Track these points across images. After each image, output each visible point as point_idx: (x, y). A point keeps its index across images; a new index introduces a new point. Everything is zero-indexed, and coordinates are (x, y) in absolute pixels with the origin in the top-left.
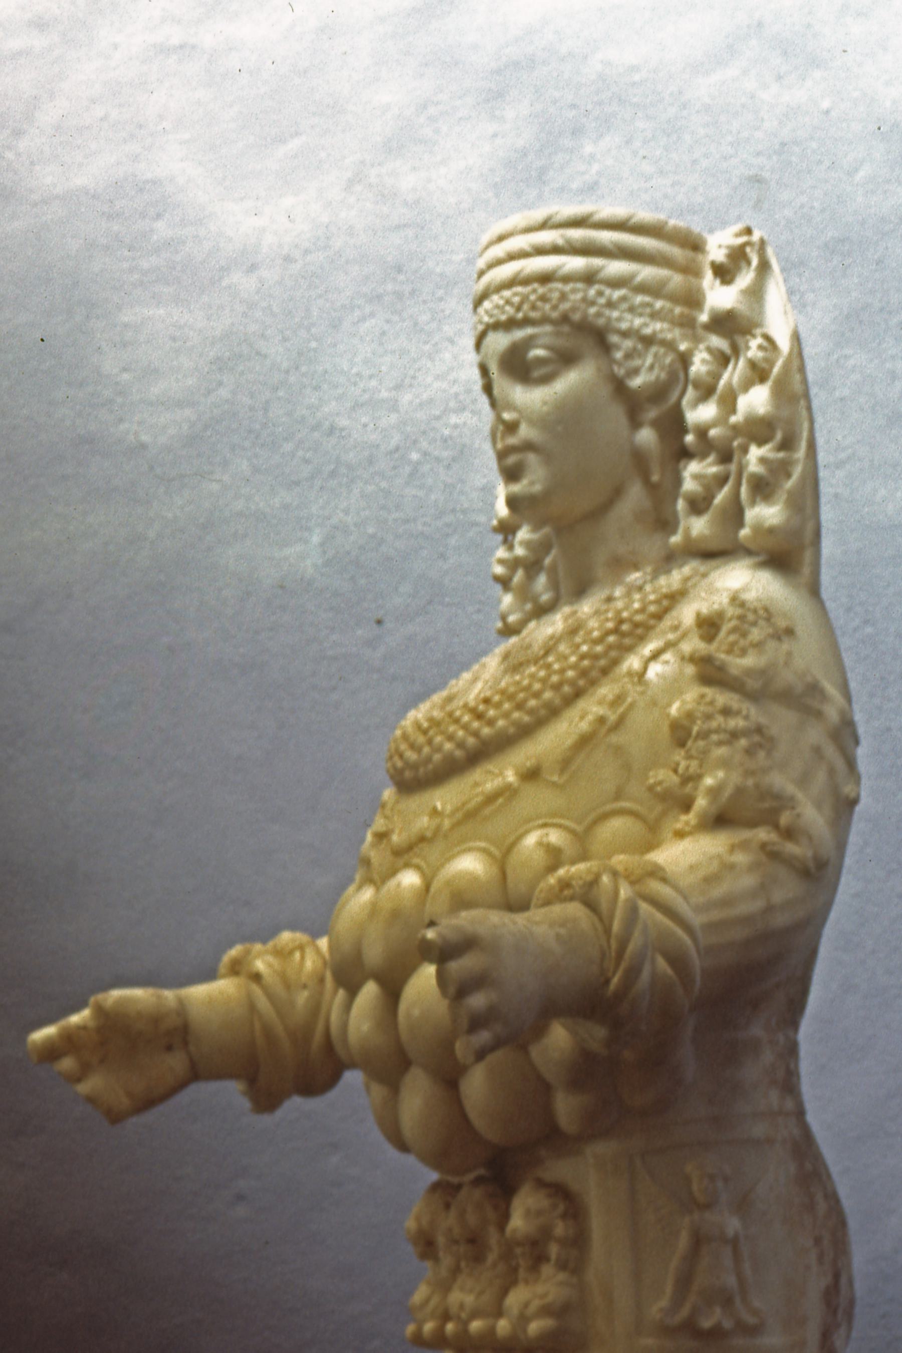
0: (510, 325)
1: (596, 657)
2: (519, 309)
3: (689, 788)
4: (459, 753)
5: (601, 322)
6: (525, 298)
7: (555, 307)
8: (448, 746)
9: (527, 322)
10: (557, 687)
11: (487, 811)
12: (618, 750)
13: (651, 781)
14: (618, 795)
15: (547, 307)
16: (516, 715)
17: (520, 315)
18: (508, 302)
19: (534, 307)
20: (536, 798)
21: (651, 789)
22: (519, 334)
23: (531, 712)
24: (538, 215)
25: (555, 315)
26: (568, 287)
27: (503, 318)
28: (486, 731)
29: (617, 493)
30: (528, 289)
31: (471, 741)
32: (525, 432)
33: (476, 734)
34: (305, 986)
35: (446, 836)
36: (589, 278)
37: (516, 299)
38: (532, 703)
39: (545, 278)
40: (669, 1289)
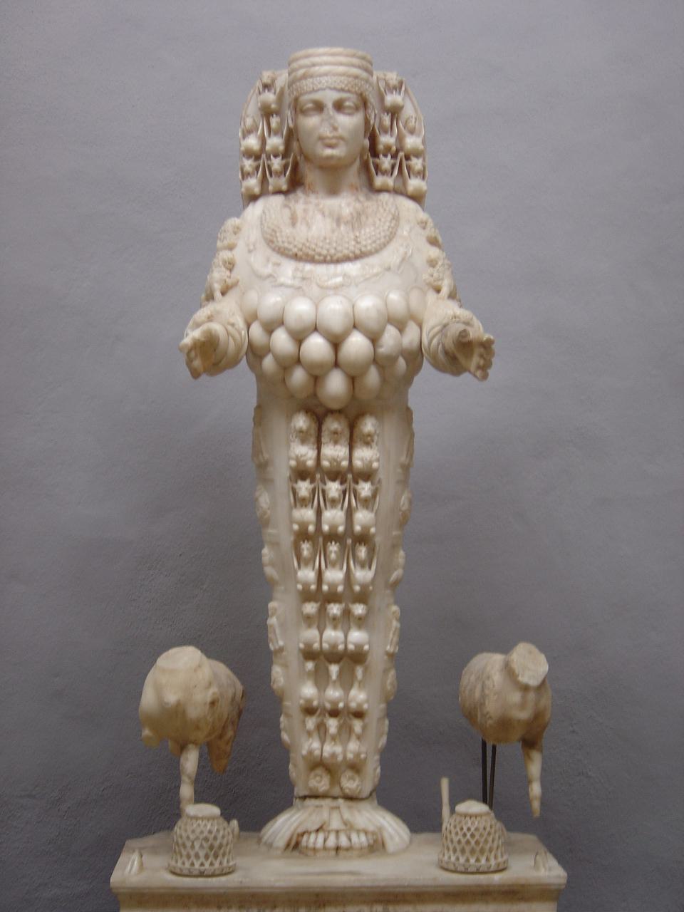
0: (342, 90)
1: (393, 228)
2: (346, 85)
3: (440, 283)
4: (351, 255)
5: (367, 97)
6: (349, 83)
7: (359, 89)
8: (346, 252)
9: (349, 91)
10: (385, 237)
13: (424, 278)
15: (357, 89)
16: (374, 245)
17: (347, 88)
18: (341, 82)
19: (352, 86)
21: (425, 281)
22: (344, 95)
23: (380, 245)
24: (360, 53)
25: (359, 92)
26: (363, 83)
27: (339, 87)
28: (363, 249)
29: (355, 160)
30: (350, 79)
31: (358, 252)
32: (340, 132)
33: (361, 250)
35: (357, 286)
36: (367, 81)
37: (346, 82)
38: (378, 242)
39: (356, 77)
40: (405, 452)
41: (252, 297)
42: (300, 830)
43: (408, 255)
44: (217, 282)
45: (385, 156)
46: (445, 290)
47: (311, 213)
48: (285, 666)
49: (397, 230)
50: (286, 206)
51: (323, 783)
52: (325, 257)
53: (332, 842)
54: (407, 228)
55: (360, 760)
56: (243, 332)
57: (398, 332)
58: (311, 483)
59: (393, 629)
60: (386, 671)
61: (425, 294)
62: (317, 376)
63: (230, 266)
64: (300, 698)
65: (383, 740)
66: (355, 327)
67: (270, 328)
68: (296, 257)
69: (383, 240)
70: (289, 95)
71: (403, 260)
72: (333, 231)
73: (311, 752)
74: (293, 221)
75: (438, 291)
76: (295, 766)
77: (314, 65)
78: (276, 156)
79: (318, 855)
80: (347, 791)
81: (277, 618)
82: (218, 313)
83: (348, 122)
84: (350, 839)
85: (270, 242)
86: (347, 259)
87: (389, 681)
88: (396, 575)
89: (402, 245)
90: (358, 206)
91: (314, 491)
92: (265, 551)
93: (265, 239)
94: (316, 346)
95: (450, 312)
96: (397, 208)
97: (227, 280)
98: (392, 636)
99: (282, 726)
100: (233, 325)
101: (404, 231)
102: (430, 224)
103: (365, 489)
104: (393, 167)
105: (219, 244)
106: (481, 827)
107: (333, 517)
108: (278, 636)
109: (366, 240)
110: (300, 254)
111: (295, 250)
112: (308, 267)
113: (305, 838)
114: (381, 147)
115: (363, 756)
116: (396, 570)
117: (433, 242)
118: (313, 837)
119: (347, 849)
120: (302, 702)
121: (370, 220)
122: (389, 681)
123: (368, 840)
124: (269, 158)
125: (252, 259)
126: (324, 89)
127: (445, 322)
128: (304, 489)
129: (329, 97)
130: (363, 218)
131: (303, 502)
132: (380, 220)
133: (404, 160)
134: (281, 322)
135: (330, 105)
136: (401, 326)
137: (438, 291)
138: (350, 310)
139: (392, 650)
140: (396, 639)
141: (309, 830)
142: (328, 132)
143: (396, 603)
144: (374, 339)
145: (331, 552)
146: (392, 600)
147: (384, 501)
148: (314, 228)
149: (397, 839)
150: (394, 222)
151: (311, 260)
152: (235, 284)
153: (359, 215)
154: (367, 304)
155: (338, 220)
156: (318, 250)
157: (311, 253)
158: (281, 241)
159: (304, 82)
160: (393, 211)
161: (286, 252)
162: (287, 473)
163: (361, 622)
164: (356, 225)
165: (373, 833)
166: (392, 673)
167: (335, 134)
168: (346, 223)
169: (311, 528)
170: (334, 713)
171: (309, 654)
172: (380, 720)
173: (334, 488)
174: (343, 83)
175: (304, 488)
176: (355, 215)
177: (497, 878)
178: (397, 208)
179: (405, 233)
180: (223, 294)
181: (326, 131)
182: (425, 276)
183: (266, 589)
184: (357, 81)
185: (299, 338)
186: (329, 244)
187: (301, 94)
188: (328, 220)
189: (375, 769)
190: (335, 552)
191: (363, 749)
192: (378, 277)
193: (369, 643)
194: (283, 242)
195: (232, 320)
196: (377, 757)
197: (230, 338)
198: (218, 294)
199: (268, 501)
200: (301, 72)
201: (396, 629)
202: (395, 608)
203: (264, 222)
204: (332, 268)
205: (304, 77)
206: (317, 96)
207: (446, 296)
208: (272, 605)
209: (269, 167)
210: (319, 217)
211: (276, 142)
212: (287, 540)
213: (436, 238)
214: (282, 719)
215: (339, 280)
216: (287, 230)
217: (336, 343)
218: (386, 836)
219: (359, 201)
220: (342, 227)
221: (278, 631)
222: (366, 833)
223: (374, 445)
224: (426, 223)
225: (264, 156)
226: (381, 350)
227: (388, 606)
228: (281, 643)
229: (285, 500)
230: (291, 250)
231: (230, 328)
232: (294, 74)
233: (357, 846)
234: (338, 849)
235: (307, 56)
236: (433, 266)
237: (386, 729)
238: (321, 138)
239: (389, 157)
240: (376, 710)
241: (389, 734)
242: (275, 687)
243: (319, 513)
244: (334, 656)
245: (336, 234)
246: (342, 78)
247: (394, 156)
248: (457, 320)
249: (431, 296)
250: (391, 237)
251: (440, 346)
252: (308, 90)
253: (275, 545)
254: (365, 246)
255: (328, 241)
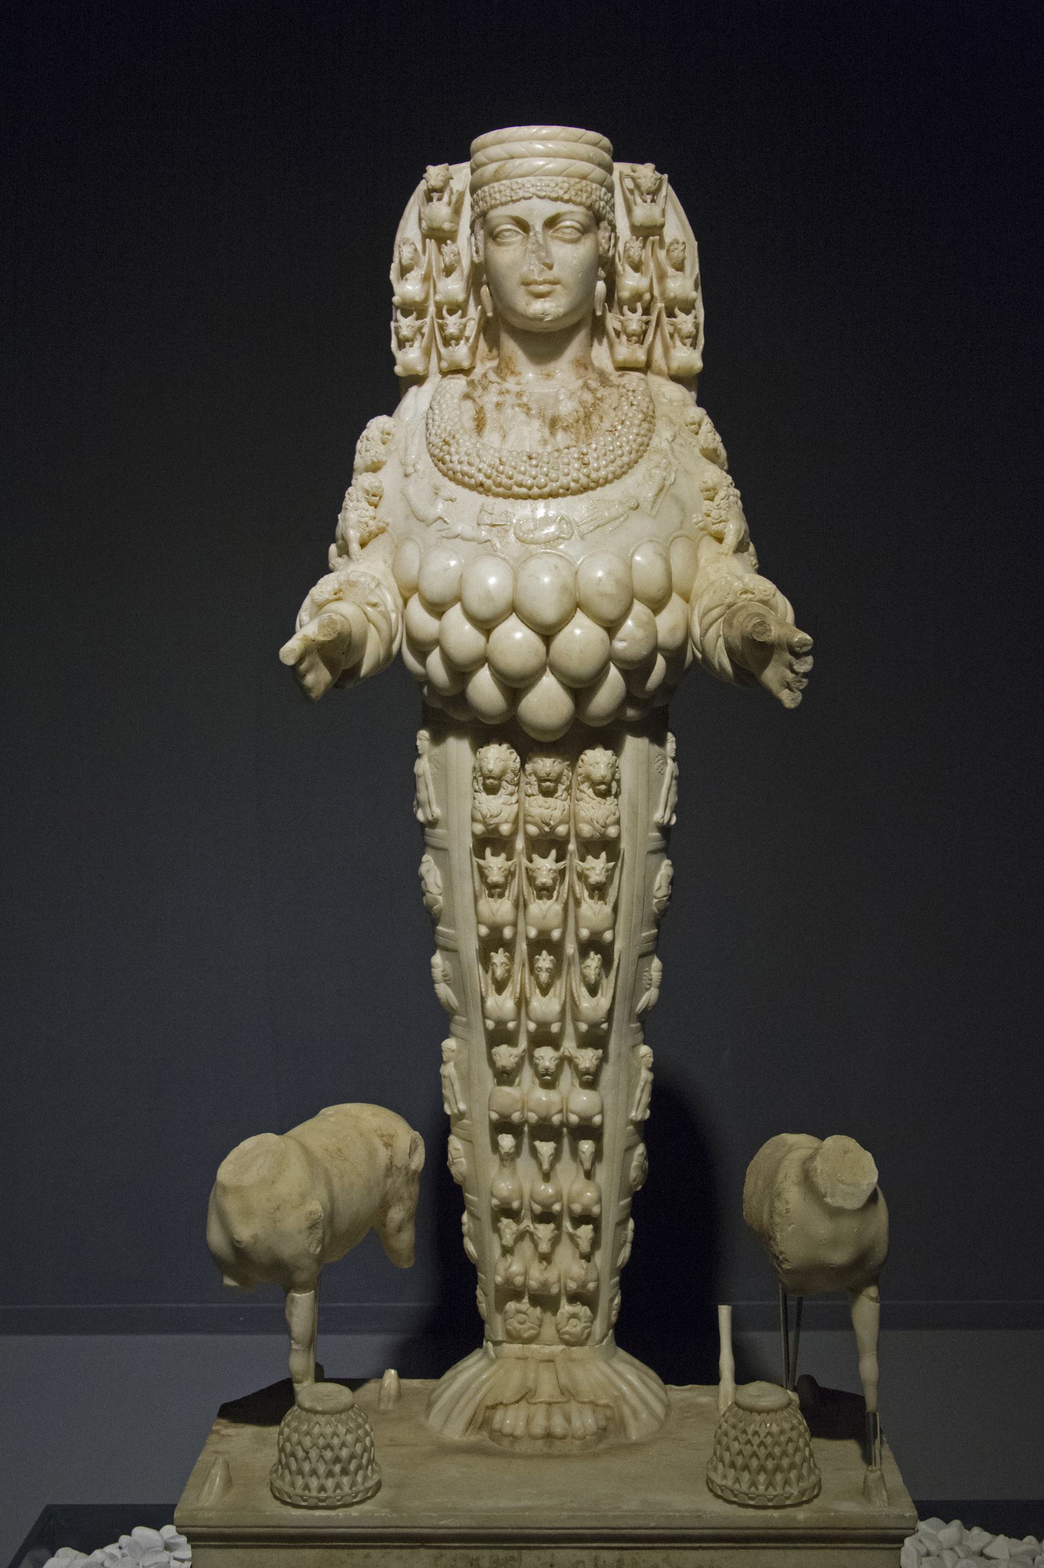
0: (556, 199)
4: (572, 485)
8: (564, 480)
9: (567, 201)
11: (609, 528)
12: (676, 499)
14: (681, 528)
15: (585, 196)
17: (566, 197)
20: (638, 524)
23: (622, 467)
26: (594, 186)
27: (554, 195)
28: (594, 475)
30: (573, 181)
31: (584, 480)
32: (555, 273)
34: (393, 611)
37: (566, 185)
38: (619, 462)
39: (584, 177)
41: (411, 553)
42: (489, 1402)
43: (668, 483)
44: (353, 528)
45: (633, 311)
46: (731, 540)
47: (509, 411)
48: (468, 1141)
49: (650, 439)
50: (467, 396)
51: (528, 1325)
52: (530, 488)
53: (538, 1426)
54: (667, 434)
55: (588, 1291)
56: (393, 616)
57: (649, 612)
58: (508, 859)
59: (642, 1083)
60: (630, 1149)
61: (695, 548)
62: (515, 687)
63: (374, 498)
64: (493, 1195)
65: (626, 1253)
66: (578, 605)
67: (437, 609)
68: (480, 487)
69: (626, 459)
70: (472, 207)
71: (661, 490)
72: (545, 442)
73: (508, 1281)
74: (480, 424)
75: (720, 540)
76: (486, 1295)
77: (512, 158)
78: (451, 312)
79: (520, 1448)
80: (567, 1337)
81: (456, 1066)
82: (352, 584)
83: (570, 256)
84: (568, 1420)
85: (439, 461)
86: (568, 491)
87: (635, 1163)
88: (649, 996)
89: (657, 467)
90: (588, 397)
91: (510, 874)
92: (437, 959)
93: (432, 455)
94: (515, 641)
95: (737, 585)
96: (651, 401)
97: (371, 522)
98: (642, 1095)
99: (465, 1229)
100: (374, 605)
101: (663, 435)
102: (707, 424)
103: (597, 867)
104: (647, 323)
105: (358, 461)
106: (775, 1429)
107: (544, 911)
108: (458, 1096)
109: (597, 459)
110: (488, 482)
111: (481, 477)
112: (501, 504)
113: (498, 1415)
114: (625, 294)
115: (591, 1286)
116: (647, 990)
117: (711, 456)
118: (512, 1412)
119: (563, 1438)
120: (495, 1201)
121: (606, 425)
122: (635, 1163)
123: (596, 1421)
124: (442, 317)
125: (411, 490)
126: (530, 198)
127: (729, 600)
128: (495, 871)
129: (538, 211)
130: (595, 420)
131: (496, 890)
132: (623, 423)
133: (664, 315)
134: (458, 598)
135: (538, 226)
136: (657, 605)
137: (720, 540)
138: (570, 580)
139: (639, 1118)
140: (646, 1099)
141: (504, 1401)
142: (536, 272)
143: (645, 1043)
144: (611, 627)
145: (541, 969)
146: (640, 1036)
147: (626, 886)
148: (512, 437)
149: (644, 1415)
150: (646, 425)
151: (509, 495)
152: (382, 531)
153: (588, 416)
154: (599, 574)
155: (553, 424)
156: (520, 477)
157: (505, 480)
158: (456, 459)
159: (496, 185)
160: (644, 405)
161: (466, 479)
162: (469, 843)
163: (591, 1081)
164: (583, 431)
165: (606, 1406)
166: (641, 1149)
167: (549, 275)
168: (565, 429)
169: (508, 932)
170: (546, 1217)
171: (502, 1125)
172: (621, 1224)
173: (545, 866)
174: (561, 188)
175: (496, 865)
176: (582, 414)
177: (801, 1515)
178: (651, 401)
179: (665, 445)
180: (363, 545)
181: (533, 269)
182: (696, 517)
183: (440, 1021)
184: (584, 183)
185: (486, 626)
186: (537, 466)
187: (492, 207)
188: (536, 424)
189: (612, 1300)
190: (547, 970)
191: (593, 1275)
192: (617, 523)
193: (602, 1112)
194: (460, 463)
195: (375, 600)
196: (617, 1279)
197: (372, 628)
198: (354, 547)
199: (440, 884)
200: (491, 168)
201: (646, 1082)
202: (645, 1050)
203: (430, 426)
204: (541, 504)
205: (496, 178)
206: (517, 210)
207: (731, 550)
208: (449, 1044)
209: (442, 328)
210: (522, 417)
211: (454, 287)
212: (470, 948)
213: (715, 450)
214: (465, 1217)
215: (552, 529)
216: (466, 443)
217: (547, 634)
218: (627, 1411)
219: (589, 389)
220: (560, 435)
221: (457, 1086)
222: (594, 1404)
223: (610, 799)
224: (700, 426)
225: (432, 310)
226: (619, 645)
227: (634, 1047)
228: (462, 1106)
229: (466, 885)
230: (471, 477)
231: (369, 609)
232: (479, 172)
233: (580, 1433)
234: (549, 1436)
235: (501, 142)
236: (712, 499)
237: (630, 1234)
238: (526, 284)
239: (640, 310)
240: (613, 1209)
241: (635, 1244)
242: (454, 1170)
243: (520, 905)
244: (545, 1130)
245: (549, 448)
246: (560, 179)
247: (647, 311)
248: (750, 596)
249: (708, 549)
250: (641, 450)
251: (721, 641)
252: (504, 199)
253: (452, 952)
254: (598, 470)
255: (534, 462)
